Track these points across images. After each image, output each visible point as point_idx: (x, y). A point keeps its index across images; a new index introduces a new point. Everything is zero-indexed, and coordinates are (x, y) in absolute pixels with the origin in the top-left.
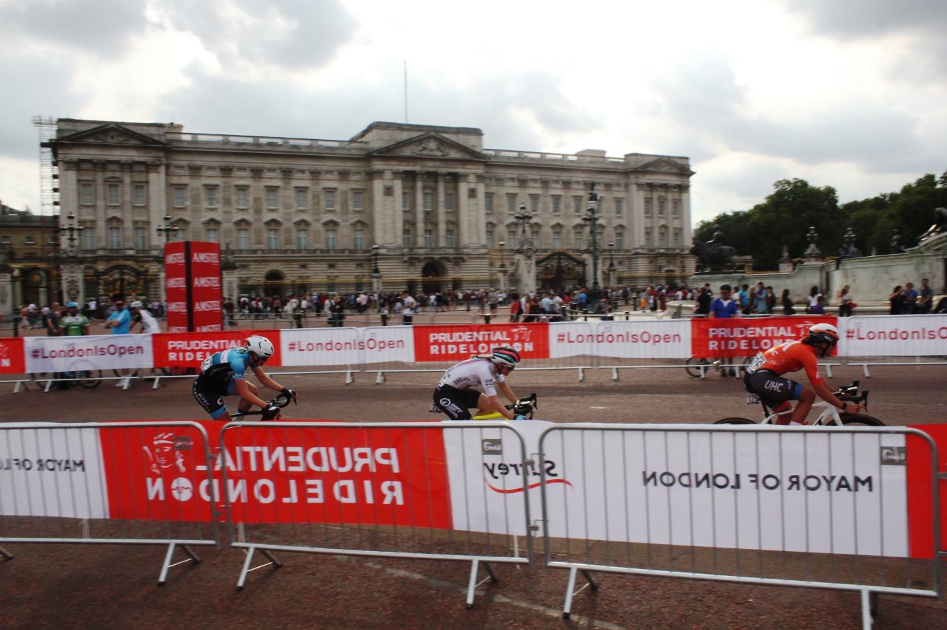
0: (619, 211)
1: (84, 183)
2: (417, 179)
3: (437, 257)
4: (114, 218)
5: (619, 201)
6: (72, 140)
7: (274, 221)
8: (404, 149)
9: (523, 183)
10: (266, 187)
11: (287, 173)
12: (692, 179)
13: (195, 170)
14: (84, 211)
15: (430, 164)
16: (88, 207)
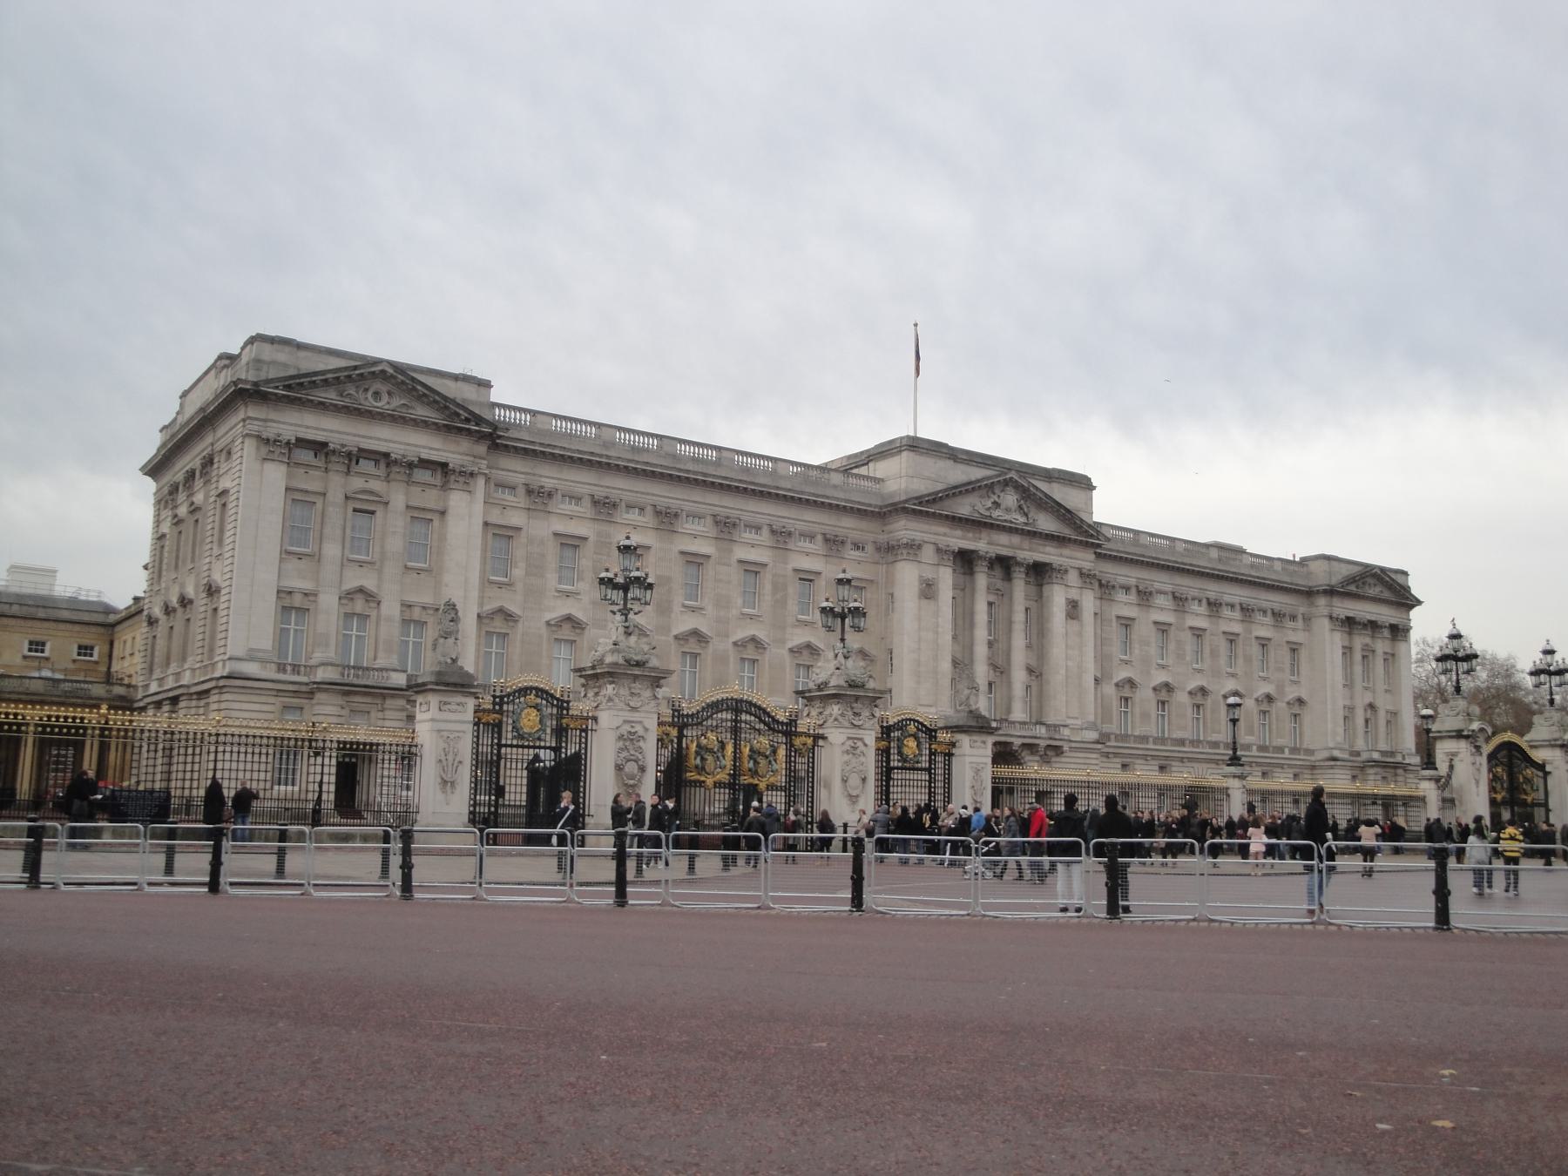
0: (1295, 667)
1: (298, 496)
2: (977, 569)
3: (1017, 742)
4: (361, 590)
5: (1294, 649)
6: (288, 387)
7: (695, 633)
8: (959, 500)
9: (1145, 596)
10: (682, 553)
11: (726, 527)
12: (1415, 614)
13: (539, 496)
14: (292, 565)
15: (1003, 538)
16: (300, 556)
